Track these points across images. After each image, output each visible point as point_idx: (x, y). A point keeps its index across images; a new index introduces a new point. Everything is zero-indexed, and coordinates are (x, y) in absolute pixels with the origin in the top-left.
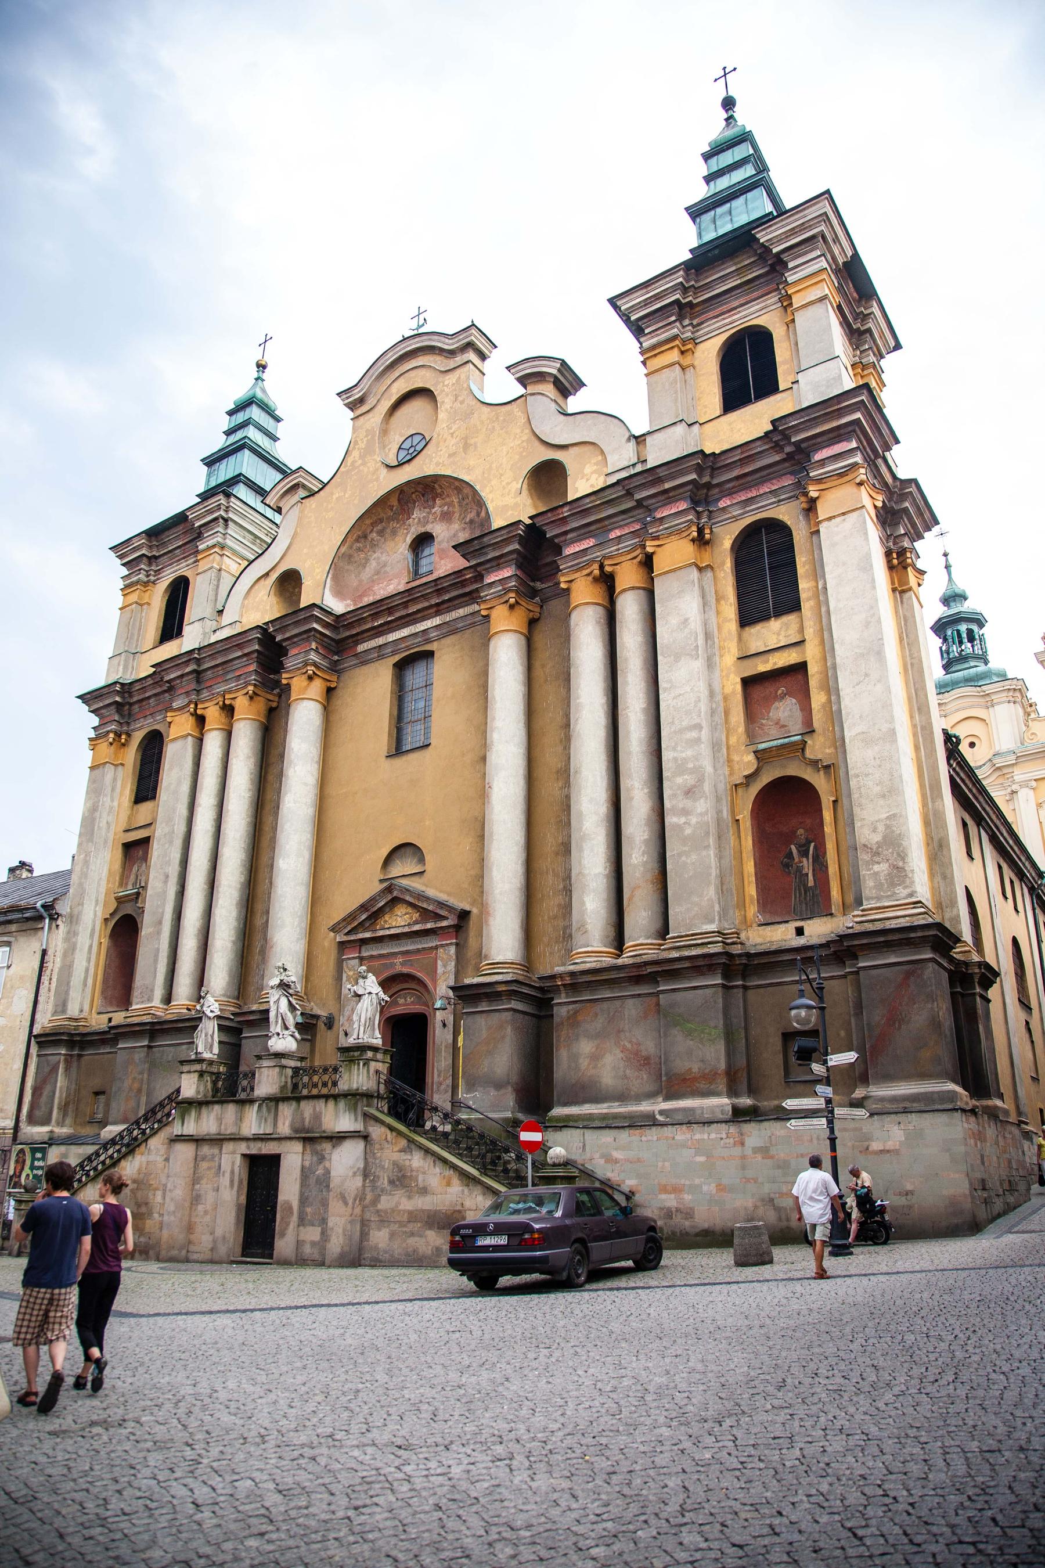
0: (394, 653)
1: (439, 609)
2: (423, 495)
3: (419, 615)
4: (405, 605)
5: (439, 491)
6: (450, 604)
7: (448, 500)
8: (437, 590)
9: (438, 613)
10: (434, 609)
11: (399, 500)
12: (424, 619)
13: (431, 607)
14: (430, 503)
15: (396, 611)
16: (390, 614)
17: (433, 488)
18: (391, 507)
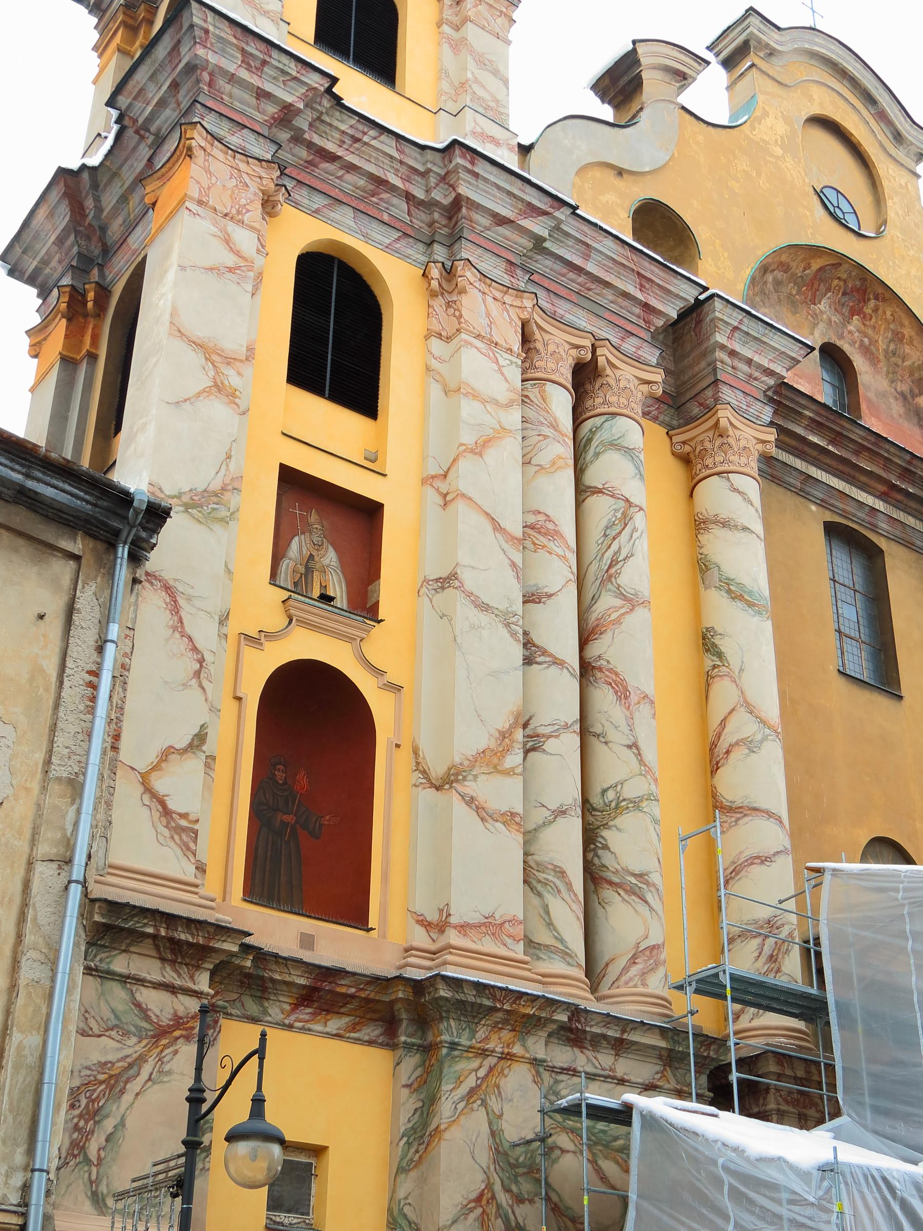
0: (823, 504)
1: (889, 493)
2: (844, 294)
3: (863, 478)
4: (860, 449)
5: (868, 310)
6: (905, 500)
7: (870, 332)
8: (906, 470)
9: (883, 496)
10: (883, 488)
11: (821, 269)
12: (863, 487)
13: (879, 478)
14: (846, 311)
15: (845, 448)
16: (831, 442)
17: (865, 301)
18: (808, 266)
